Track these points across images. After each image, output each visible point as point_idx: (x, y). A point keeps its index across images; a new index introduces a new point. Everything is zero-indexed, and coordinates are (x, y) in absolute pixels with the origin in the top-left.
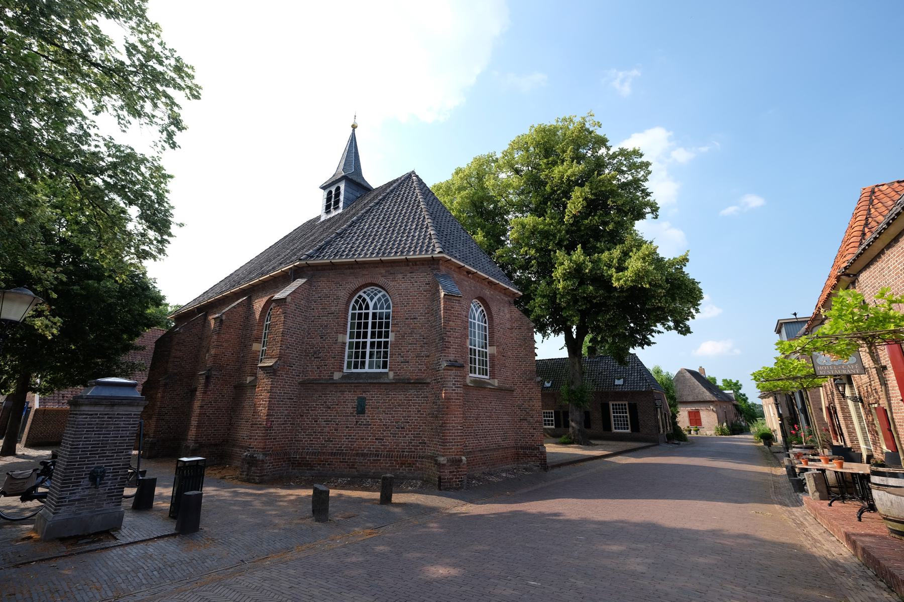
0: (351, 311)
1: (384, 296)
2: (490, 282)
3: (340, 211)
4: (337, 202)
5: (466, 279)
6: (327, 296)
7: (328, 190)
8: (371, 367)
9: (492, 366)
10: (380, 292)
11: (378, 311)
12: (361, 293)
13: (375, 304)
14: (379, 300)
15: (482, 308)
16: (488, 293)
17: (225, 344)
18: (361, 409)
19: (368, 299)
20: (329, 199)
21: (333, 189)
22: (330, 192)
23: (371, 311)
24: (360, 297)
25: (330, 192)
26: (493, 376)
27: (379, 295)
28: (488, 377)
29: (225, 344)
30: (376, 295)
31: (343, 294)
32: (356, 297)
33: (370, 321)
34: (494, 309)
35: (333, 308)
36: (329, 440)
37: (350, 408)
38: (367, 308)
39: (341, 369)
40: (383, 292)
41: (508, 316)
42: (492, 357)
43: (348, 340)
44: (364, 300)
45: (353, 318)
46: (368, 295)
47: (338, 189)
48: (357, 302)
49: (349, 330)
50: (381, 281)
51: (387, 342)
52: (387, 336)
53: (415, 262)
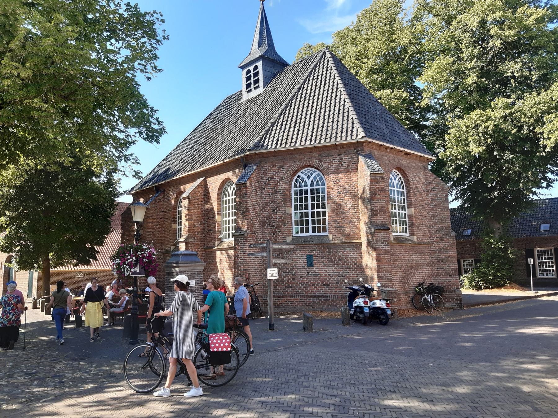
0: (293, 189)
1: (318, 175)
2: (407, 154)
3: (261, 90)
4: (256, 82)
5: (386, 154)
6: (273, 178)
7: (246, 70)
8: (314, 231)
9: (411, 225)
10: (315, 172)
12: (299, 174)
13: (312, 181)
15: (400, 176)
17: (194, 217)
18: (310, 263)
20: (248, 79)
21: (251, 68)
22: (249, 72)
23: (309, 188)
24: (299, 177)
25: (249, 72)
27: (315, 174)
28: (408, 234)
29: (194, 217)
31: (285, 175)
32: (296, 177)
33: (309, 195)
34: (411, 176)
35: (280, 188)
36: (289, 286)
37: (302, 262)
38: (306, 185)
39: (290, 234)
40: (318, 172)
41: (423, 180)
42: (411, 217)
43: (293, 212)
45: (296, 194)
46: (306, 175)
47: (256, 67)
48: (296, 180)
49: (293, 204)
50: (316, 162)
52: (324, 207)
53: (342, 146)
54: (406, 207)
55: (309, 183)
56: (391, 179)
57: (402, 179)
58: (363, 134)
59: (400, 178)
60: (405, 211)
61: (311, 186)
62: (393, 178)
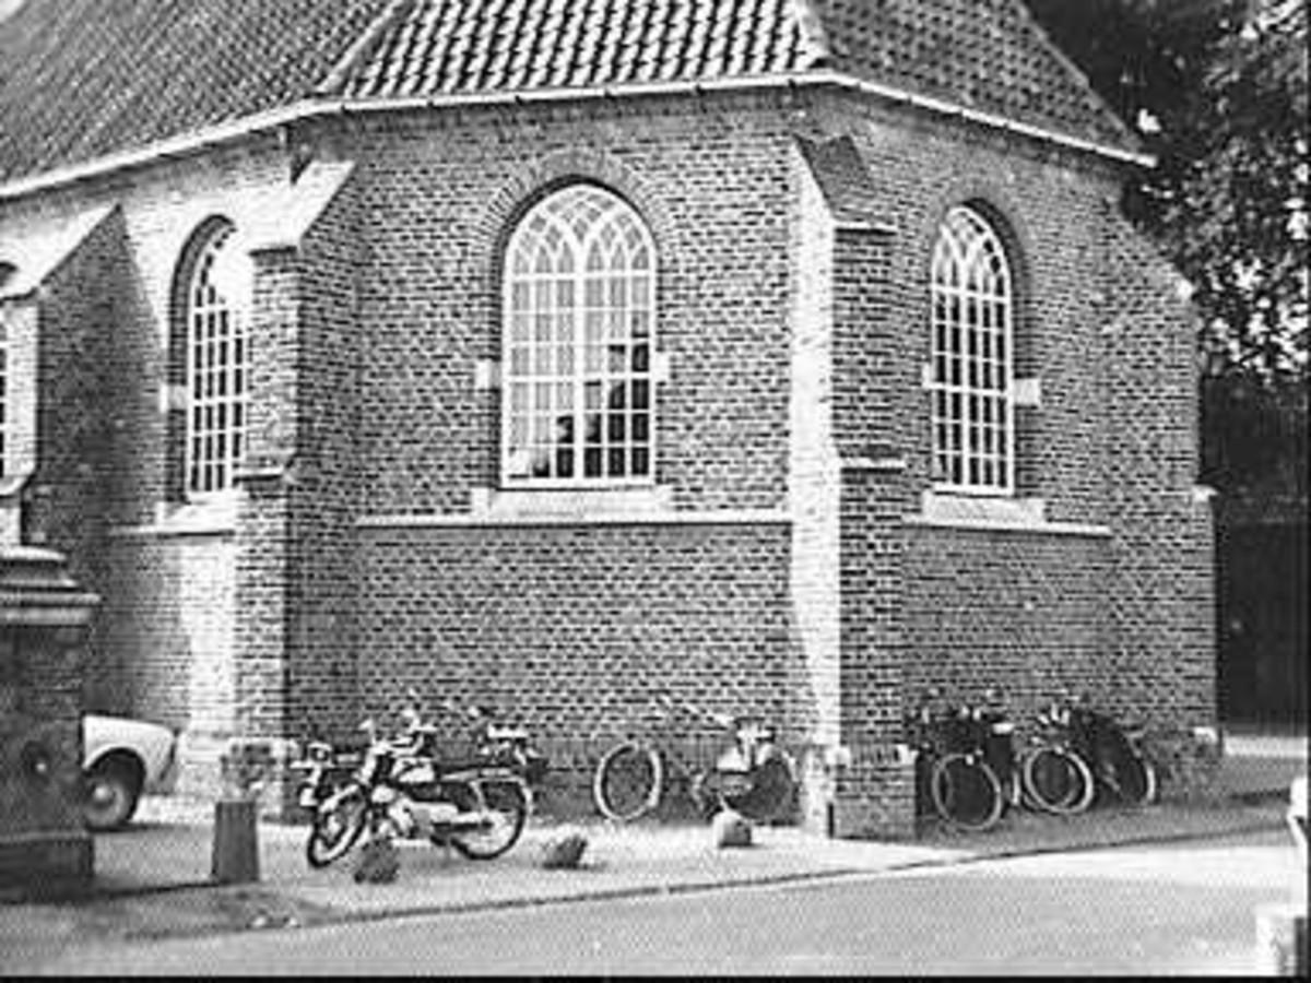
10: (608, 205)
11: (605, 274)
12: (540, 209)
14: (608, 233)
15: (989, 234)
16: (1002, 176)
19: (567, 232)
26: (1025, 490)
27: (608, 216)
30: (594, 215)
31: (478, 217)
38: (567, 264)
40: (621, 207)
44: (555, 234)
51: (645, 383)
54: (1009, 373)
55: (581, 254)
56: (947, 250)
57: (999, 252)
58: (817, 51)
59: (988, 246)
60: (1002, 387)
61: (590, 268)
62: (953, 243)
